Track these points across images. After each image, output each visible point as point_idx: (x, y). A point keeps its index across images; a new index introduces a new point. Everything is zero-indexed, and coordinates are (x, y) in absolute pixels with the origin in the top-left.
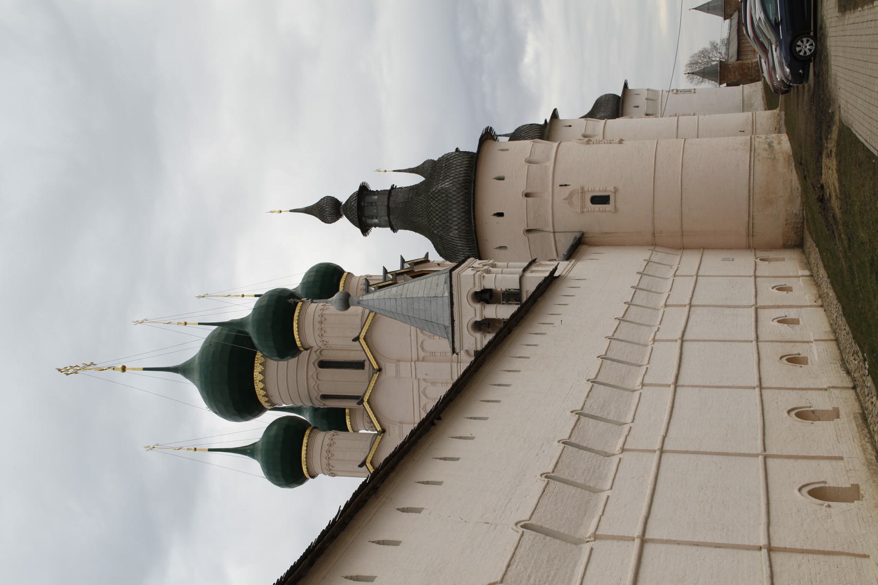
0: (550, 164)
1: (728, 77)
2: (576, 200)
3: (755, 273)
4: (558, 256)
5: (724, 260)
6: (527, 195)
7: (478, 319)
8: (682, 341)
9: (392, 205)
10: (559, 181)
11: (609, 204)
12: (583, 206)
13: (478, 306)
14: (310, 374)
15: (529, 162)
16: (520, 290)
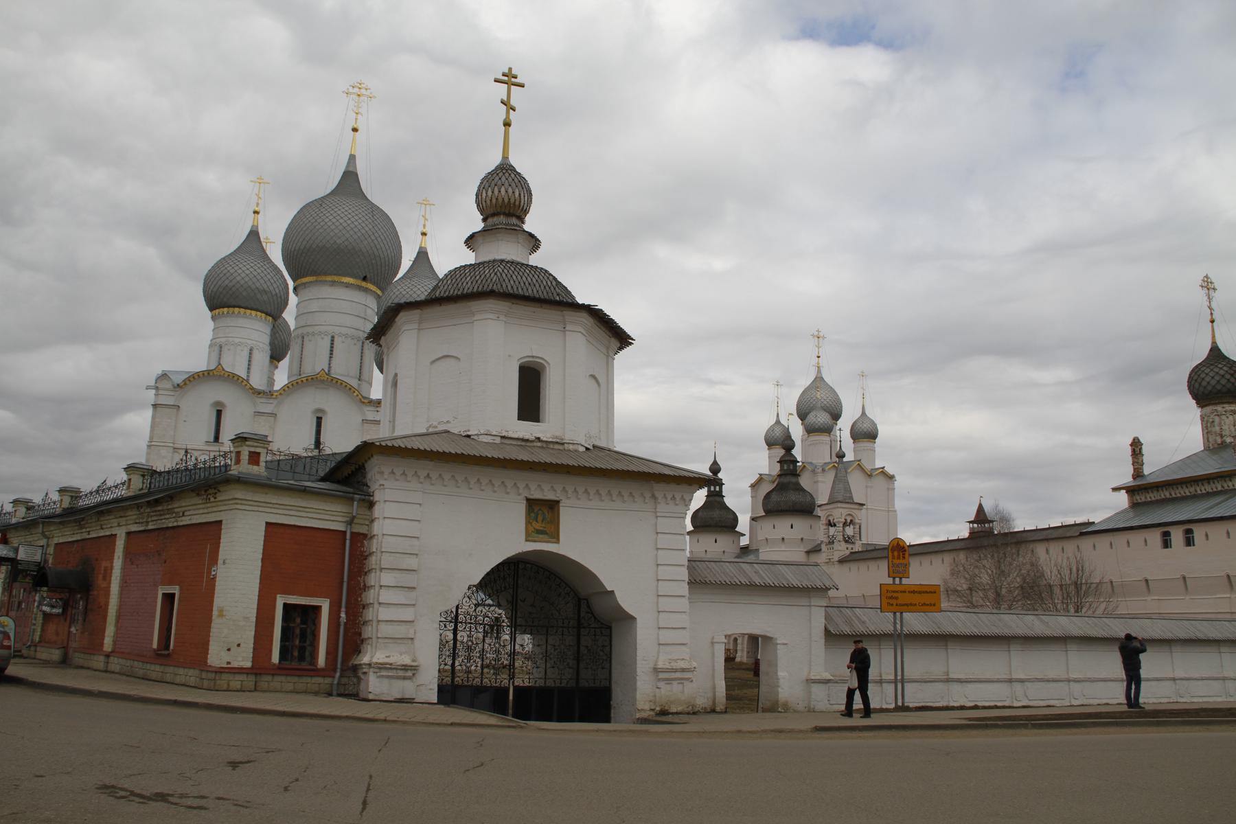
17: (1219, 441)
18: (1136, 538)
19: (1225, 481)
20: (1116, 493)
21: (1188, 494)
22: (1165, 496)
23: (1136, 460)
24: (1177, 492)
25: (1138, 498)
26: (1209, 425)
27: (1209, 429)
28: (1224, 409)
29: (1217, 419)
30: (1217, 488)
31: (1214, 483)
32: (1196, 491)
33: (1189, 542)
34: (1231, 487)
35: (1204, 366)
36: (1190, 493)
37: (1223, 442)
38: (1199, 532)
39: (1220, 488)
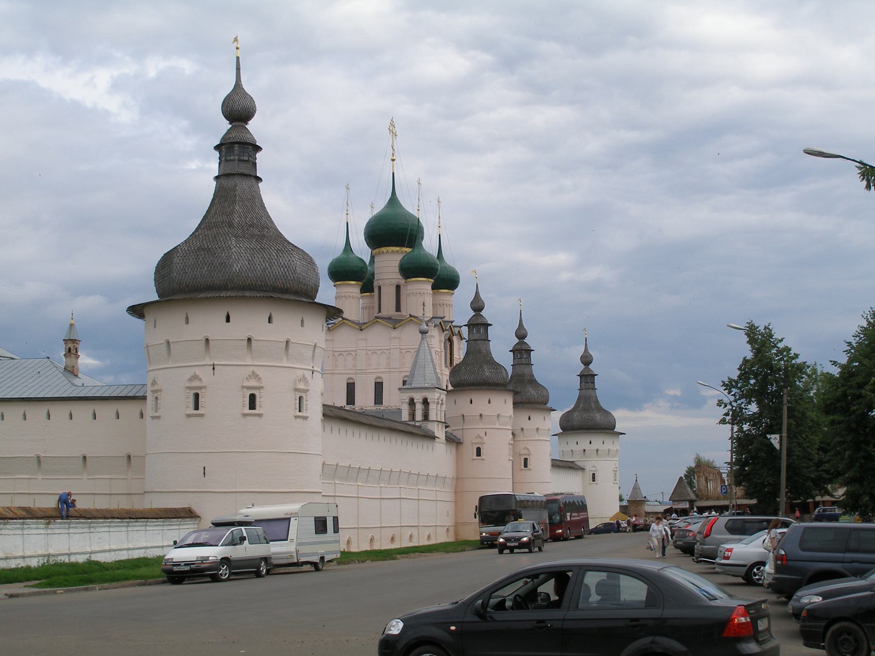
0: (498, 426)
1: (633, 506)
2: (479, 440)
3: (438, 526)
4: (453, 430)
5: (448, 512)
6: (481, 415)
8: (400, 498)
9: (479, 342)
10: (487, 431)
11: (477, 456)
12: (475, 443)
13: (421, 400)
14: (392, 280)
15: (498, 416)
16: (429, 421)
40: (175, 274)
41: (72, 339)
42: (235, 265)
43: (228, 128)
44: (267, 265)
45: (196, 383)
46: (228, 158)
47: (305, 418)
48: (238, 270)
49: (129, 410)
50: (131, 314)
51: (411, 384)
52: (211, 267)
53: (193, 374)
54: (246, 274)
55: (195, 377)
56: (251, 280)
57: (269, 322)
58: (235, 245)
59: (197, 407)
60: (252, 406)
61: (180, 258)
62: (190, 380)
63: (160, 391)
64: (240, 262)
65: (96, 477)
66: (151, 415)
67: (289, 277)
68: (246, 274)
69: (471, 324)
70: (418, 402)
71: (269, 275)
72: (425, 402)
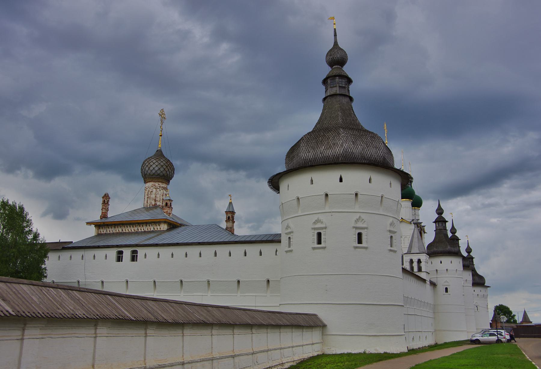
7: (413, 261)
12: (444, 285)
13: (417, 260)
17: (153, 203)
18: (100, 253)
19: (156, 226)
20: (88, 226)
21: (133, 231)
22: (119, 230)
23: (104, 207)
24: (127, 229)
25: (102, 231)
26: (149, 193)
27: (149, 196)
28: (159, 185)
29: (154, 190)
30: (150, 229)
31: (149, 226)
32: (138, 230)
33: (134, 258)
34: (159, 229)
35: (153, 158)
36: (134, 230)
37: (155, 204)
38: (141, 252)
39: (152, 229)
40: (302, 153)
41: (230, 211)
42: (344, 144)
43: (330, 71)
44: (365, 146)
45: (319, 225)
46: (332, 86)
47: (395, 251)
48: (346, 148)
49: (268, 249)
50: (270, 185)
51: (411, 252)
52: (327, 147)
53: (316, 219)
54: (352, 151)
55: (317, 221)
56: (355, 156)
57: (369, 183)
58: (343, 132)
59: (319, 242)
60: (360, 241)
61: (305, 143)
62: (315, 223)
63: (292, 232)
64: (347, 143)
65: (246, 294)
66: (286, 250)
67: (379, 155)
68: (352, 151)
69: (437, 221)
70: (415, 261)
71: (366, 153)
72: (419, 261)
